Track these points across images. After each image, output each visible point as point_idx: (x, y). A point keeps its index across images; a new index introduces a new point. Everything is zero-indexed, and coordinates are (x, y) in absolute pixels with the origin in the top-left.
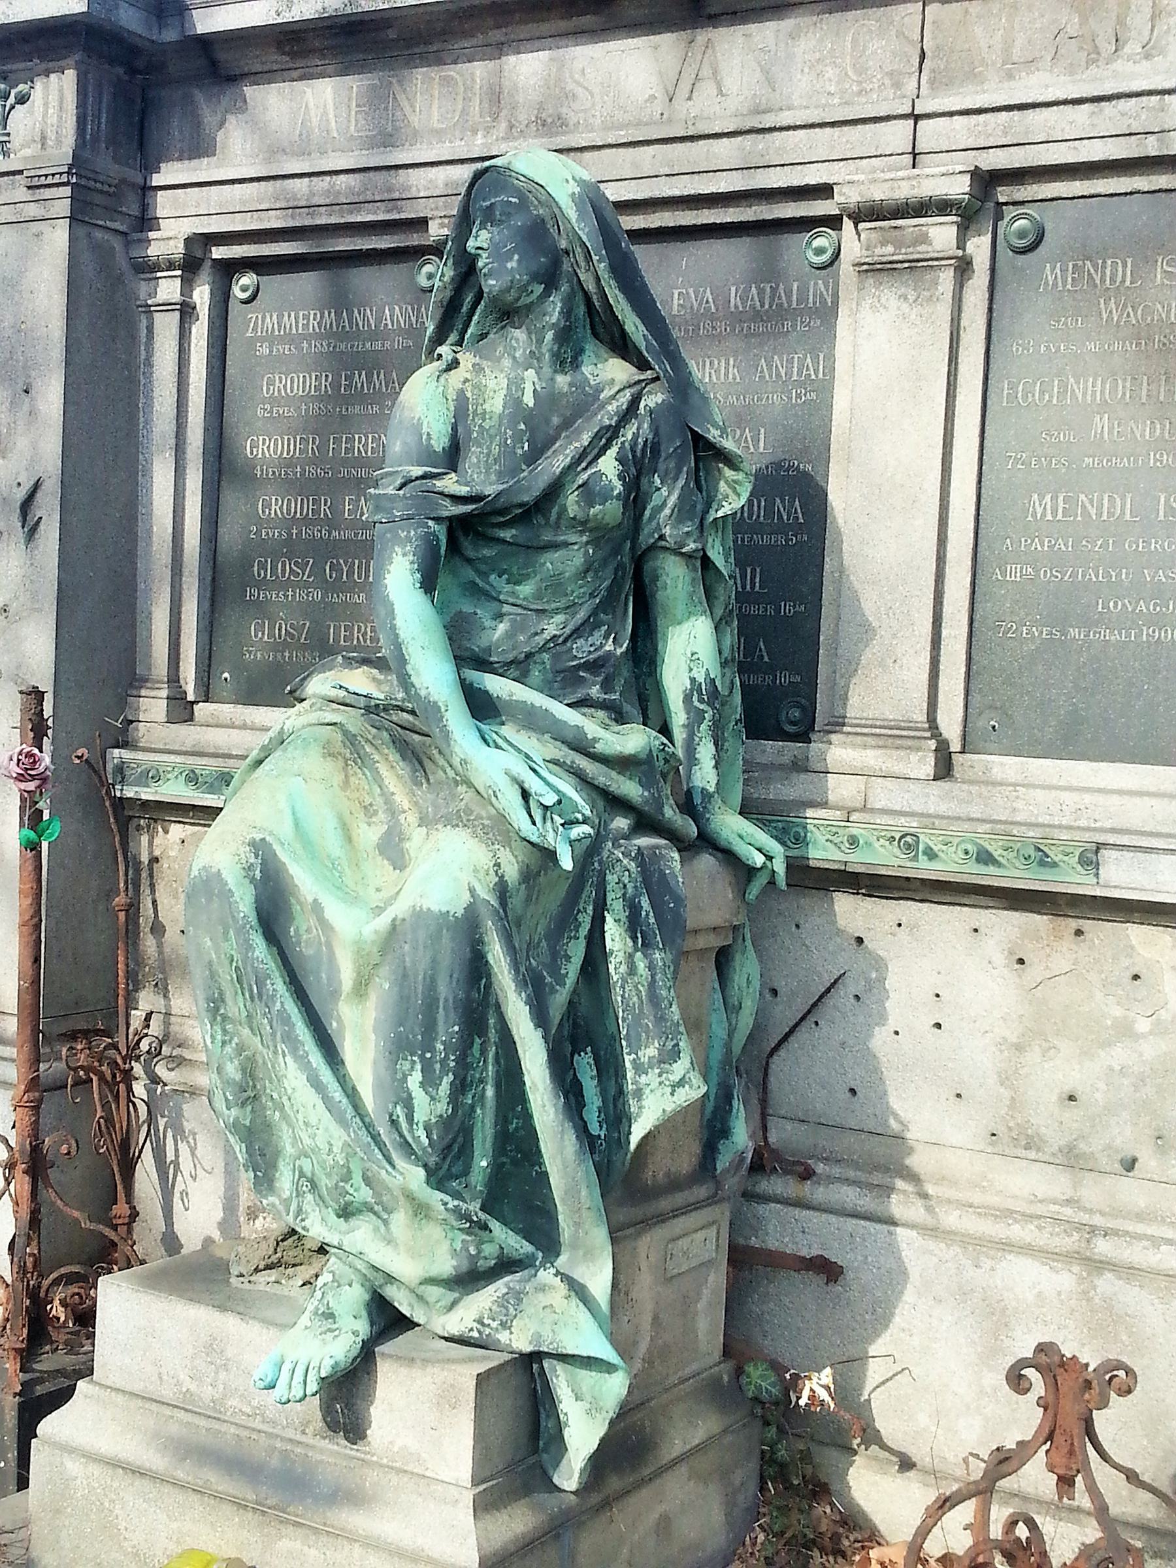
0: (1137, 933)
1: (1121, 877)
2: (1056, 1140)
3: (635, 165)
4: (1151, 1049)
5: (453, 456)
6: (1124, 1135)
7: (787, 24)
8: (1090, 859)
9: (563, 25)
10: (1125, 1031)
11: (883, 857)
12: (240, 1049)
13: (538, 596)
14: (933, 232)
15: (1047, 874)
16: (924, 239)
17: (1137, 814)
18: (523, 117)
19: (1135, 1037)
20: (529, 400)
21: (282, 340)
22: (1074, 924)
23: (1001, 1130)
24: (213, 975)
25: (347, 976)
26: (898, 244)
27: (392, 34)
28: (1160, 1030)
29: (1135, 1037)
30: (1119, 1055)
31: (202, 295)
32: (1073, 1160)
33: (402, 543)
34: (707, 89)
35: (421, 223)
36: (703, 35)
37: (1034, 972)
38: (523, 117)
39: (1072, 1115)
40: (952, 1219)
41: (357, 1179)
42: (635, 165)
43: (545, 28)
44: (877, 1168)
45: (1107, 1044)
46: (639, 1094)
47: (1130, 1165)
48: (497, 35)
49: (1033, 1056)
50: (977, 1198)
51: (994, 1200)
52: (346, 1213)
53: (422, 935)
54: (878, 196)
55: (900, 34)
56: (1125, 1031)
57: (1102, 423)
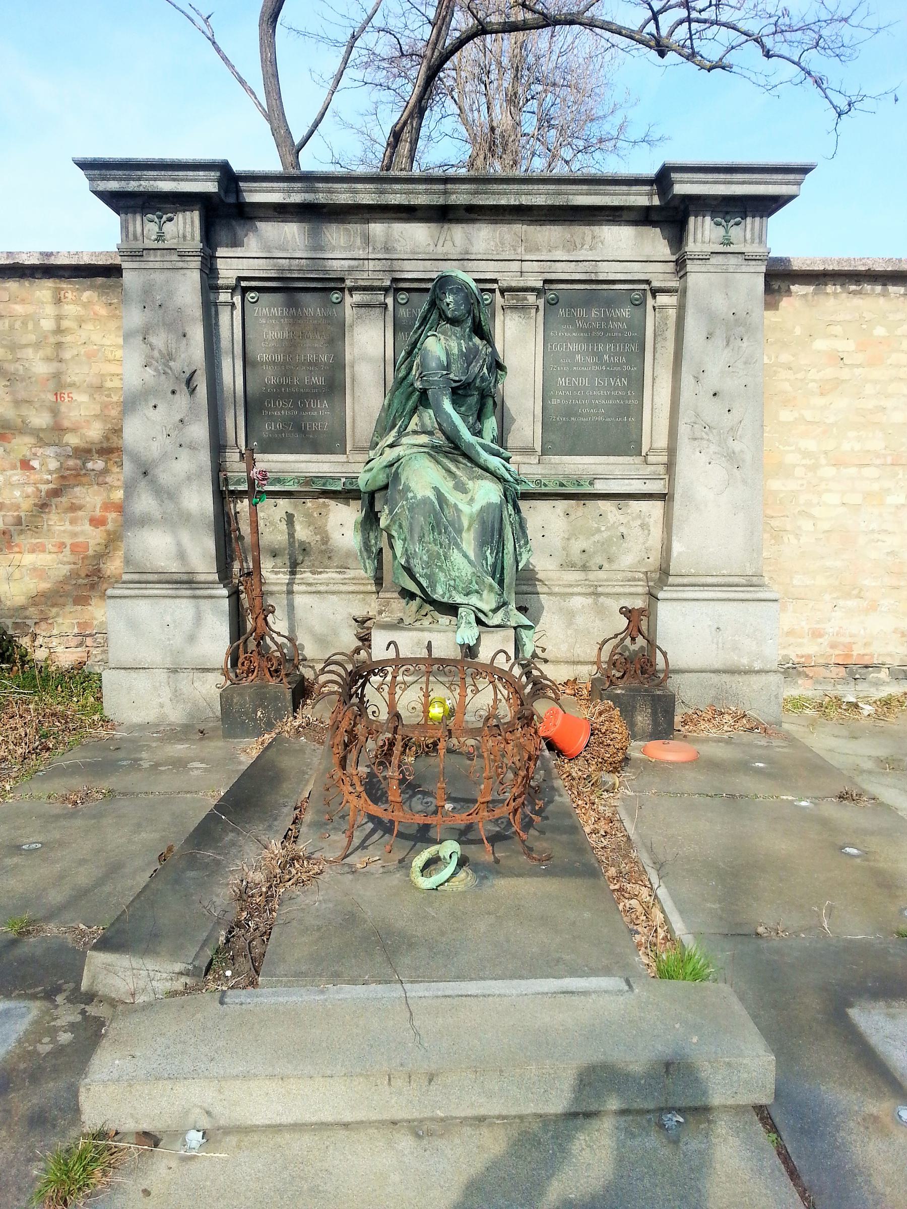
0: (600, 503)
1: (600, 487)
2: (580, 564)
3: (424, 267)
4: (605, 535)
5: (448, 368)
6: (599, 560)
7: (477, 226)
8: (591, 484)
9: (394, 215)
10: (598, 530)
11: (532, 487)
12: (428, 551)
13: (466, 411)
14: (528, 297)
15: (580, 488)
16: (526, 299)
17: (600, 469)
18: (379, 246)
19: (601, 532)
20: (464, 350)
21: (271, 318)
22: (583, 502)
23: (564, 564)
24: (422, 528)
25: (466, 524)
26: (518, 301)
27: (325, 210)
28: (608, 529)
29: (601, 532)
30: (597, 537)
31: (237, 299)
32: (585, 568)
33: (446, 395)
34: (449, 244)
35: (342, 280)
36: (446, 226)
37: (572, 517)
38: (379, 246)
39: (584, 556)
40: (556, 590)
41: (474, 583)
42: (424, 267)
43: (386, 216)
44: (528, 580)
45: (593, 535)
46: (521, 554)
47: (601, 568)
48: (368, 216)
49: (573, 541)
50: (561, 583)
51: (566, 583)
52: (467, 595)
53: (491, 511)
54: (513, 285)
55: (515, 234)
56: (598, 530)
57: (578, 357)
